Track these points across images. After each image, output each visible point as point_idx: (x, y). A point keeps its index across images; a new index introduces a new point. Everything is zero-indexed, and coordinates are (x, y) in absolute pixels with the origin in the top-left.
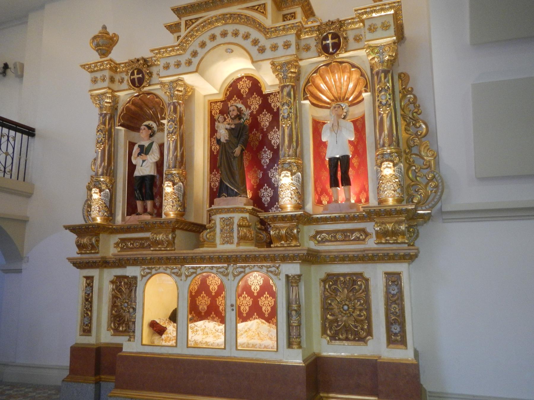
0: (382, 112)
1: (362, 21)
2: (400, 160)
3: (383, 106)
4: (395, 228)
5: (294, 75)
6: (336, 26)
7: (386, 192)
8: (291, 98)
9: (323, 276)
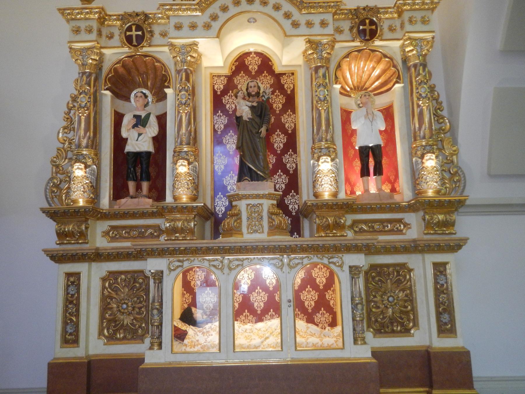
0: (181, 111)
1: (168, 18)
2: (195, 159)
4: (184, 225)
5: (95, 63)
6: (141, 19)
7: (180, 190)
8: (90, 87)
9: (104, 274)
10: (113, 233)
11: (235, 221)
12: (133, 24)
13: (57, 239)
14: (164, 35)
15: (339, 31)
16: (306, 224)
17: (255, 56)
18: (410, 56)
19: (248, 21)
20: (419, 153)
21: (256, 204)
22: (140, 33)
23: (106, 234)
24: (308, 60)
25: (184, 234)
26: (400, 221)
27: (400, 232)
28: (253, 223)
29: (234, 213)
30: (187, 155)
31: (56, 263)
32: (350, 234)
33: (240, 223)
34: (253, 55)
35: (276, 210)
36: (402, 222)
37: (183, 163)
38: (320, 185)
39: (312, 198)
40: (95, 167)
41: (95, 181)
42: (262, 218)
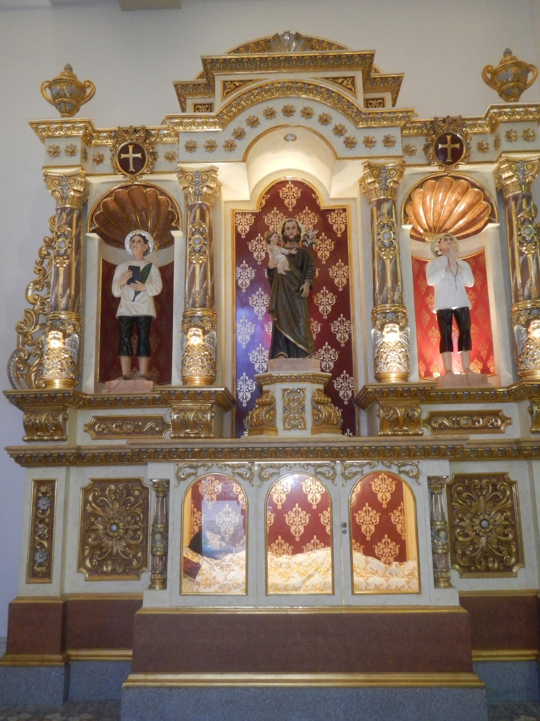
0: (194, 262)
1: (177, 135)
2: (212, 326)
3: (196, 253)
4: (197, 417)
6: (140, 136)
7: (191, 369)
8: (72, 228)
9: (87, 483)
10: (99, 427)
11: (267, 412)
12: (130, 144)
13: (23, 433)
14: (171, 158)
15: (409, 151)
16: (362, 418)
17: (292, 186)
18: (508, 185)
19: (285, 139)
20: (523, 319)
21: (296, 389)
22: (139, 155)
23: (90, 427)
24: (366, 191)
25: (197, 429)
26: (496, 414)
27: (496, 429)
28: (292, 415)
29: (266, 401)
30: (202, 321)
31: (22, 466)
32: (426, 432)
33: (274, 416)
34: (290, 185)
35: (323, 398)
36: (499, 416)
37: (196, 332)
38: (384, 364)
39: (372, 381)
40: (77, 336)
41: (76, 356)
42: (303, 408)
